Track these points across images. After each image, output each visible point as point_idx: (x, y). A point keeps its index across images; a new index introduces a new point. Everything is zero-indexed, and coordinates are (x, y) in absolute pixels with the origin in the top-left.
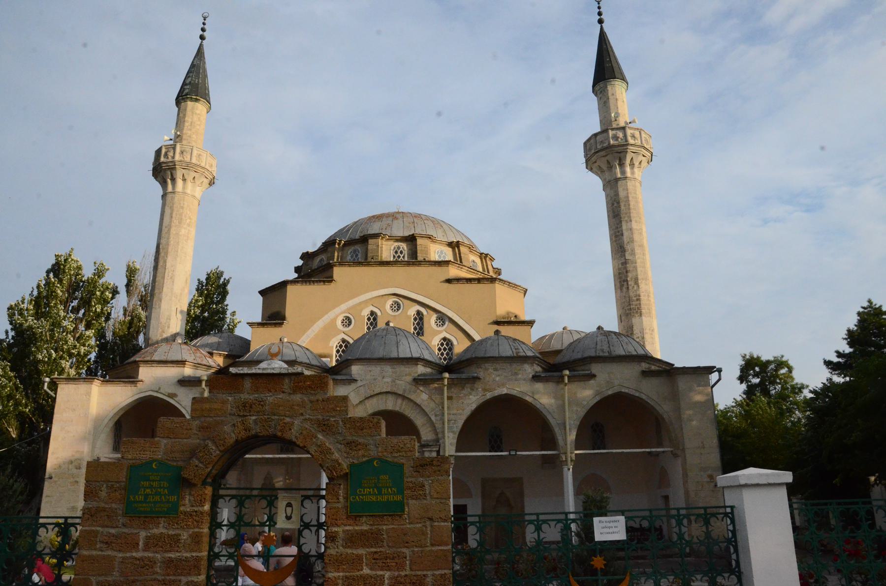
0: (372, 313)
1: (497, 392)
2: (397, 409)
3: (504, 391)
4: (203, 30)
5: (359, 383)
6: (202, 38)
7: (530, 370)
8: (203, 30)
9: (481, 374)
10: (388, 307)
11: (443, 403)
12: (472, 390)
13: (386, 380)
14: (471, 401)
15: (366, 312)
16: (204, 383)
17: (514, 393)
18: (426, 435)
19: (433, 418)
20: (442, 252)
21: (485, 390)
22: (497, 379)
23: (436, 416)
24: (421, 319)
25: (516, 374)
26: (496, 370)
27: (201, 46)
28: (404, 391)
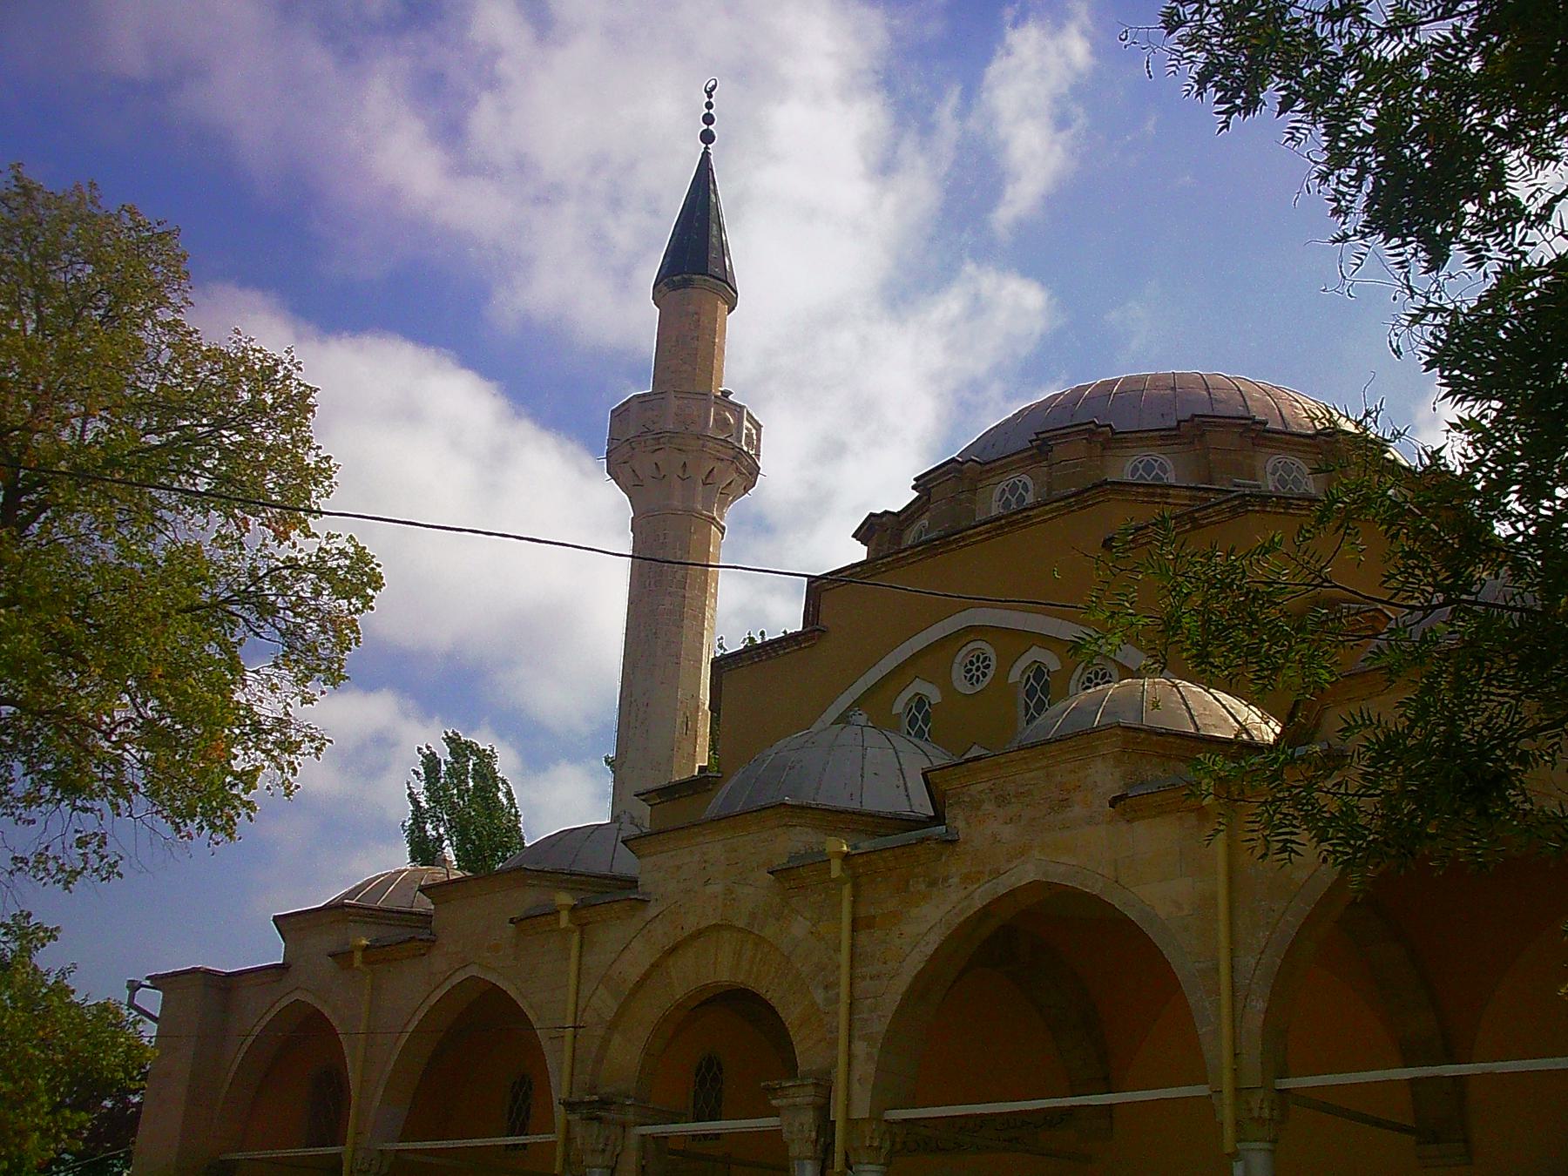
0: (921, 701)
1: (1004, 885)
2: (741, 978)
3: (1025, 873)
4: (708, 119)
5: (652, 911)
6: (707, 137)
7: (1105, 777)
8: (708, 119)
9: (960, 824)
10: (958, 673)
11: (838, 950)
12: (932, 884)
13: (709, 889)
14: (927, 923)
15: (898, 707)
16: (358, 956)
17: (1057, 875)
18: (808, 1055)
19: (819, 996)
20: (1149, 468)
21: (967, 879)
22: (1007, 832)
23: (826, 987)
24: (1046, 689)
25: (1065, 803)
26: (1002, 800)
27: (706, 154)
28: (753, 915)
